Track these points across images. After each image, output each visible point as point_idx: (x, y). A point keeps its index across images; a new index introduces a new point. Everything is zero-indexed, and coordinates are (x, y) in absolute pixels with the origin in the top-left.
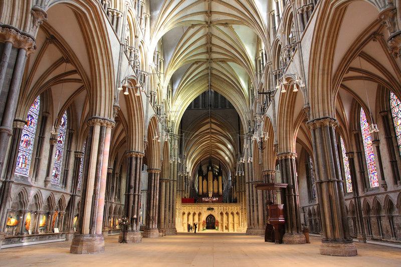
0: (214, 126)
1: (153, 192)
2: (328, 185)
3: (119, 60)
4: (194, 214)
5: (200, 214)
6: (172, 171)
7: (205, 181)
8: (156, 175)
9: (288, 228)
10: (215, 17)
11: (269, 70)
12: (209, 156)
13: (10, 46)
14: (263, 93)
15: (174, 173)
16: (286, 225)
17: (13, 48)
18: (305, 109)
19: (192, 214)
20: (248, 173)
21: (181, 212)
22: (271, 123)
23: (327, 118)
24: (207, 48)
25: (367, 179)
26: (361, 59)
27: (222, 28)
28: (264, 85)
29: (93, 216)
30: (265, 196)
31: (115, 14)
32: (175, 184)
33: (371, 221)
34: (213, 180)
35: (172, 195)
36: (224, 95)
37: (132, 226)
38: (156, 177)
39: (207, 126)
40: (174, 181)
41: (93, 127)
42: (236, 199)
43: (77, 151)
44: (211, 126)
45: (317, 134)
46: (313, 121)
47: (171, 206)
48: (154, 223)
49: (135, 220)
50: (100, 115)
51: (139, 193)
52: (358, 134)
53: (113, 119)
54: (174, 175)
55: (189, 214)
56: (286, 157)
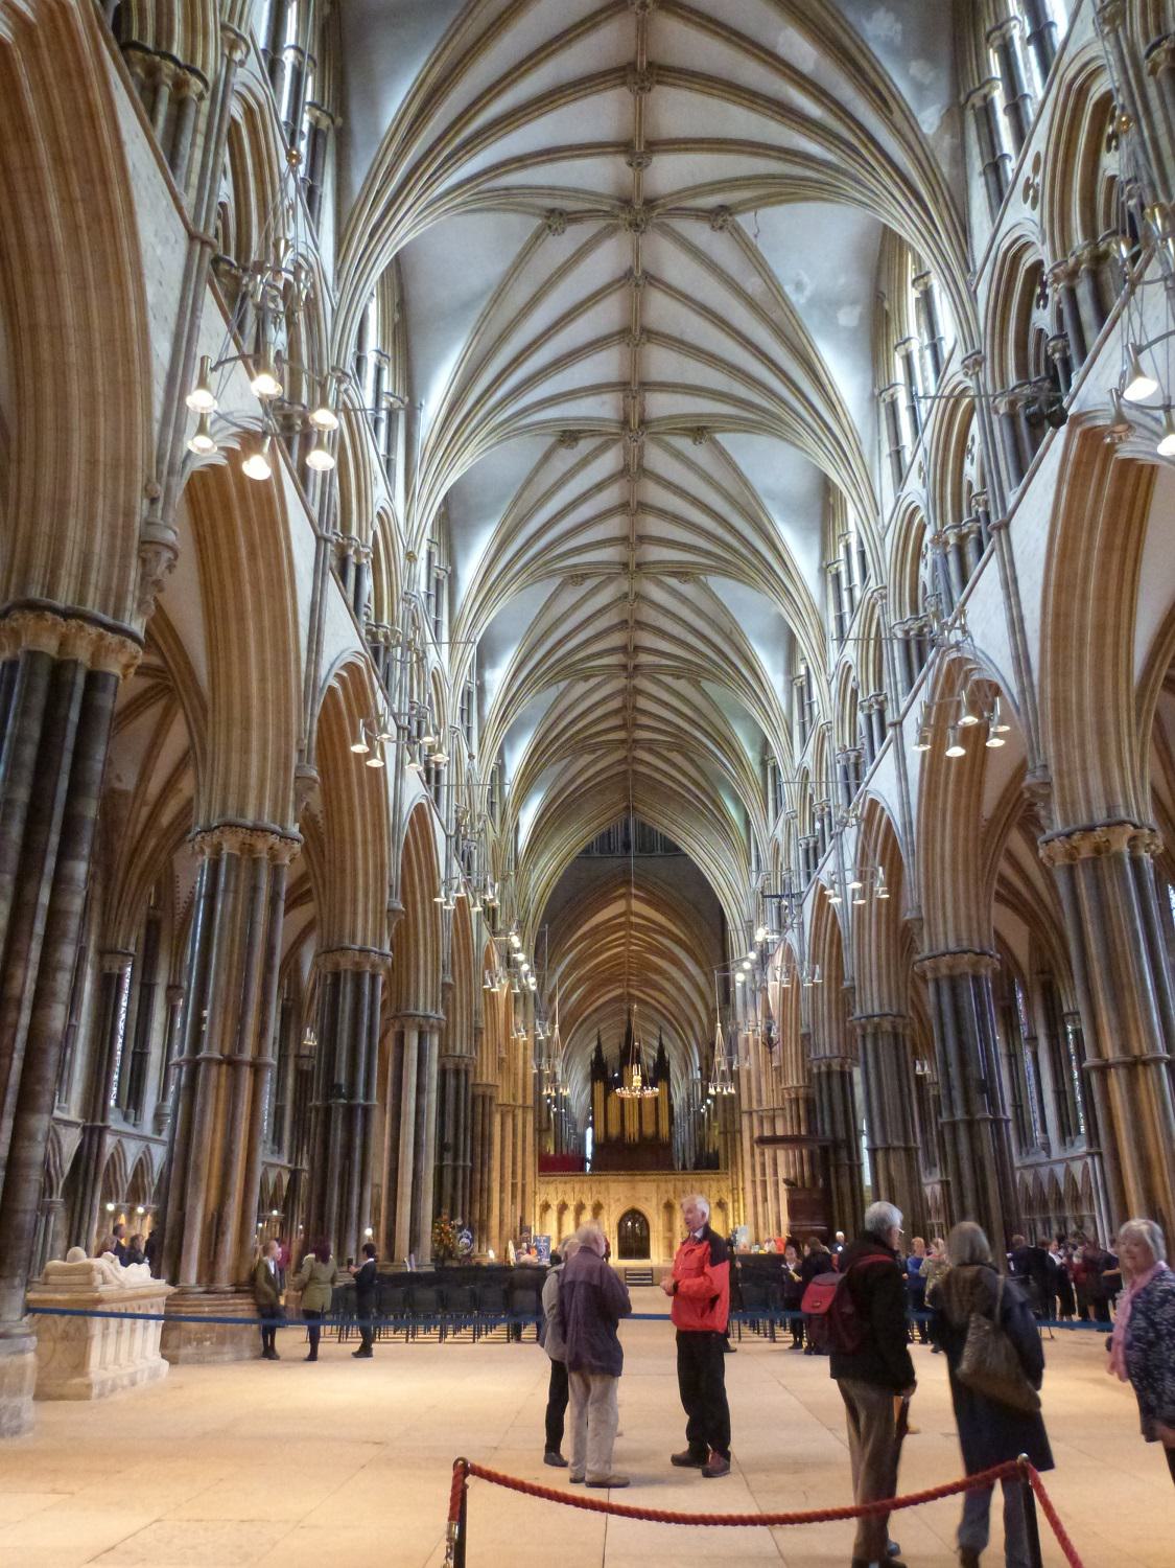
0: (637, 906)
5: (597, 1209)
10: (644, 658)
12: (618, 991)
19: (572, 1208)
20: (749, 1081)
21: (538, 1203)
23: (886, 1015)
24: (624, 719)
25: (1027, 1125)
27: (668, 680)
31: (433, 766)
32: (530, 1118)
35: (519, 1153)
36: (672, 837)
38: (487, 1106)
40: (524, 1108)
42: (716, 1154)
45: (869, 1046)
50: (417, 1009)
51: (464, 1161)
52: (1010, 1008)
53: (441, 1014)
54: (524, 1089)
55: (563, 1208)
56: (829, 1066)
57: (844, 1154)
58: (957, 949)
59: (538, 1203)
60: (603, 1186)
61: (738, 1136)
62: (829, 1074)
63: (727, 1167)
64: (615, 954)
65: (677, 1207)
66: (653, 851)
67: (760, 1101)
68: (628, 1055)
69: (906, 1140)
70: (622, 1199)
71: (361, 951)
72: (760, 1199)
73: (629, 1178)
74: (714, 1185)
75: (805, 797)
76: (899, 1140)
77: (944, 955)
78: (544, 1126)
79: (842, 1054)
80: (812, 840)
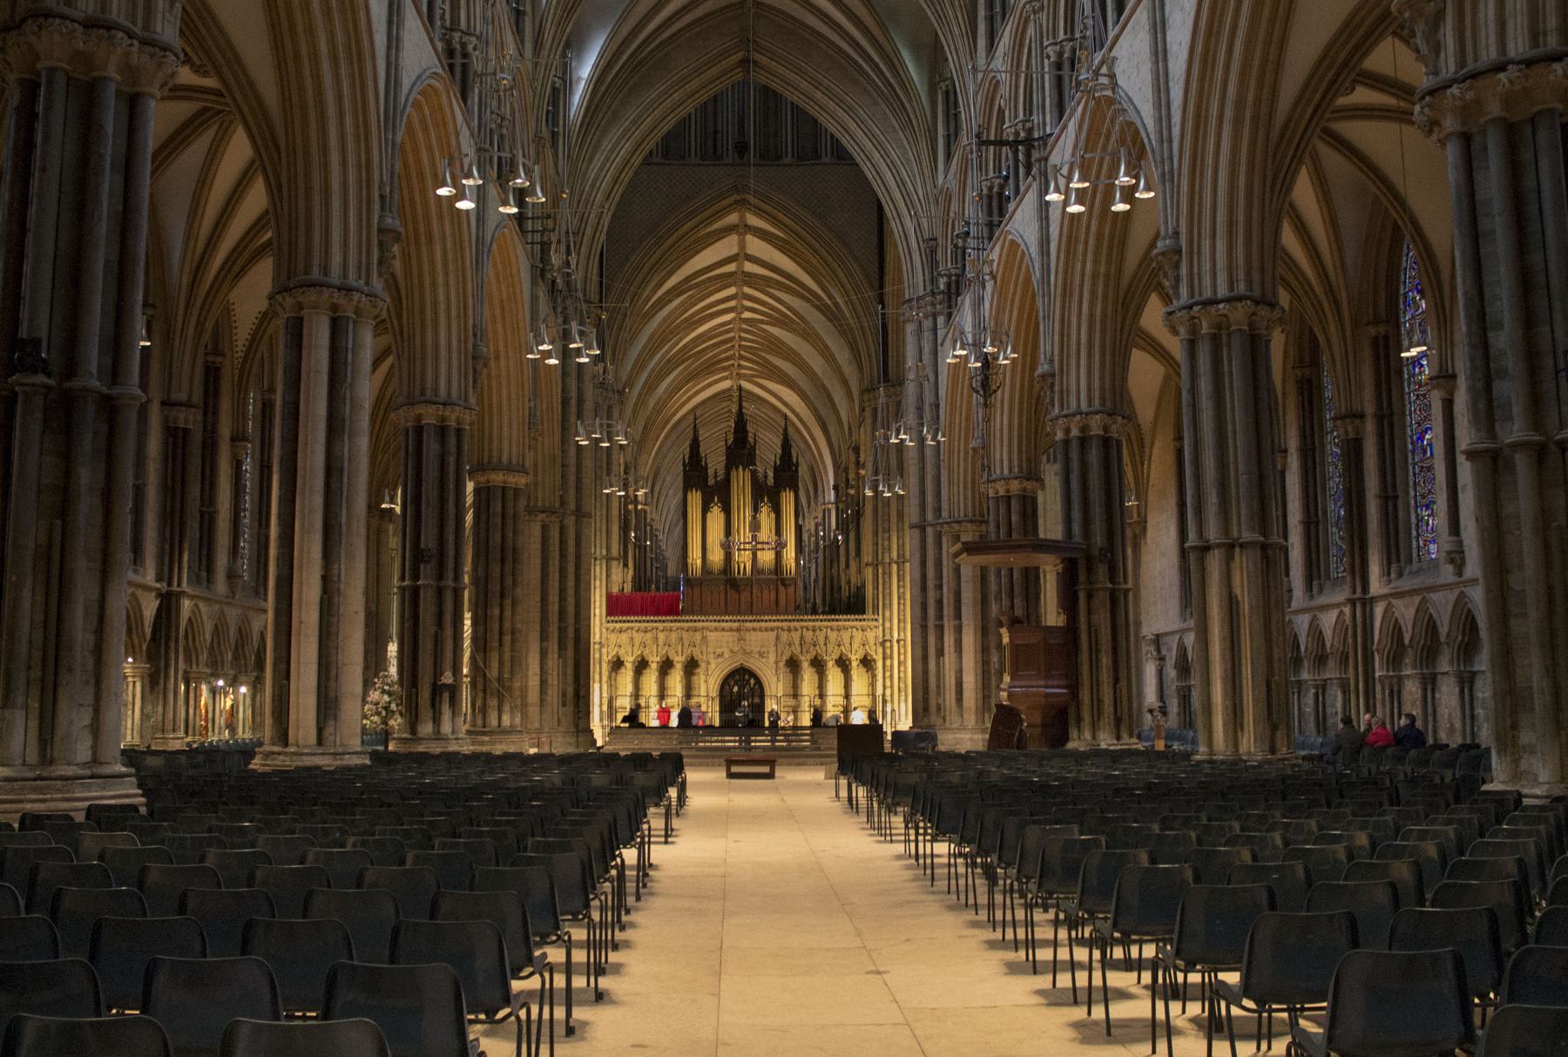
0: (755, 246)
1: (498, 569)
2: (1229, 559)
3: (390, 22)
4: (666, 666)
5: (691, 667)
6: (573, 469)
7: (716, 518)
8: (510, 495)
9: (1079, 720)
11: (1031, 31)
12: (726, 384)
13: (110, 92)
14: (1000, 143)
15: (579, 481)
16: (1072, 711)
17: (119, 93)
18: (1163, 254)
19: (654, 666)
22: (1028, 280)
23: (1240, 299)
26: (1397, 42)
28: (1004, 90)
29: (328, 679)
30: (993, 587)
33: (1405, 693)
34: (756, 509)
35: (571, 583)
36: (813, 111)
37: (437, 720)
38: (510, 504)
39: (726, 247)
41: (301, 319)
43: (174, 397)
44: (742, 245)
46: (1190, 308)
47: (571, 630)
48: (506, 707)
49: (446, 696)
50: (326, 270)
52: (1386, 338)
56: (1084, 429)
57: (1102, 570)
58: (1531, 53)
59: (605, 658)
60: (698, 636)
61: (895, 567)
62: (1084, 441)
63: (876, 610)
64: (723, 324)
65: (805, 665)
66: (779, 157)
67: (938, 510)
68: (741, 450)
69: (1264, 530)
70: (726, 656)
71: (90, 24)
72: (932, 651)
73: (737, 624)
74: (858, 635)
75: (1021, 45)
76: (1253, 530)
77: (1501, 67)
78: (615, 551)
79: (1108, 404)
80: (1068, 46)
